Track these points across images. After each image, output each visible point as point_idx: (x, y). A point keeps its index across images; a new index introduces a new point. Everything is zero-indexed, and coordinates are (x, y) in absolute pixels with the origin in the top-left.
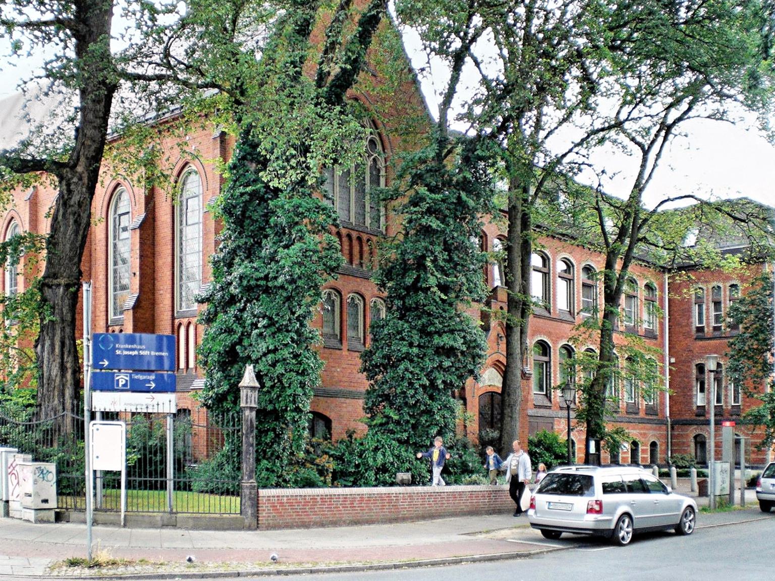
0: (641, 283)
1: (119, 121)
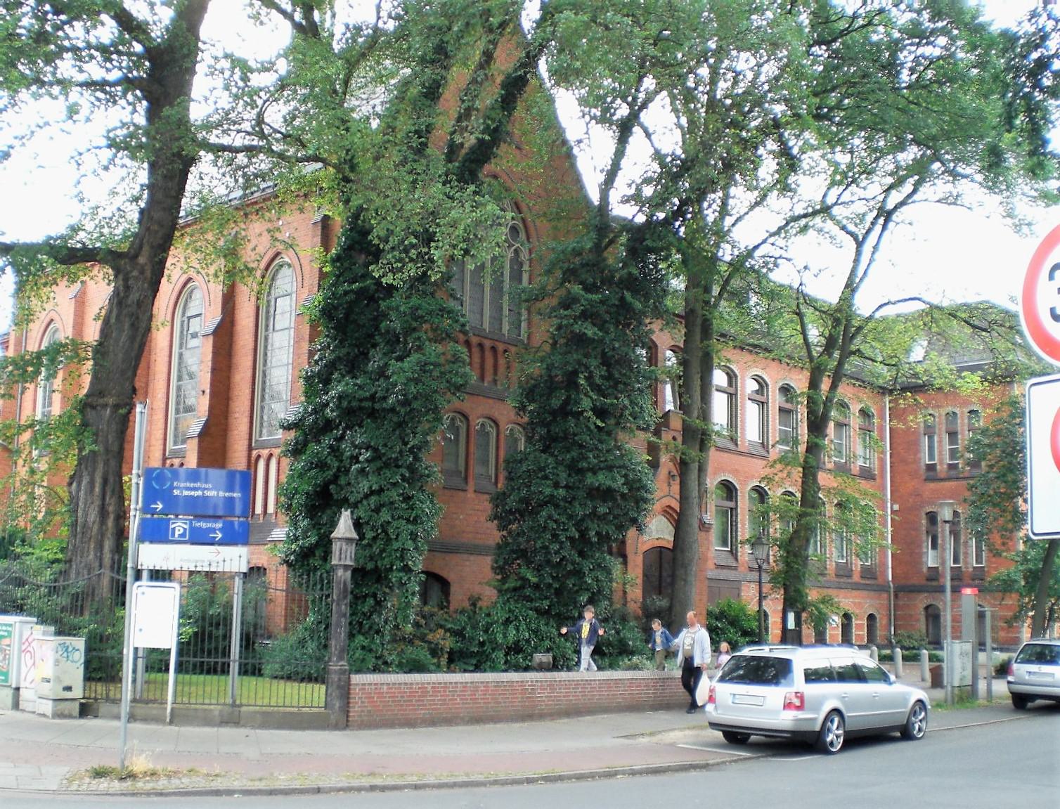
0: (855, 408)
1: (196, 201)
